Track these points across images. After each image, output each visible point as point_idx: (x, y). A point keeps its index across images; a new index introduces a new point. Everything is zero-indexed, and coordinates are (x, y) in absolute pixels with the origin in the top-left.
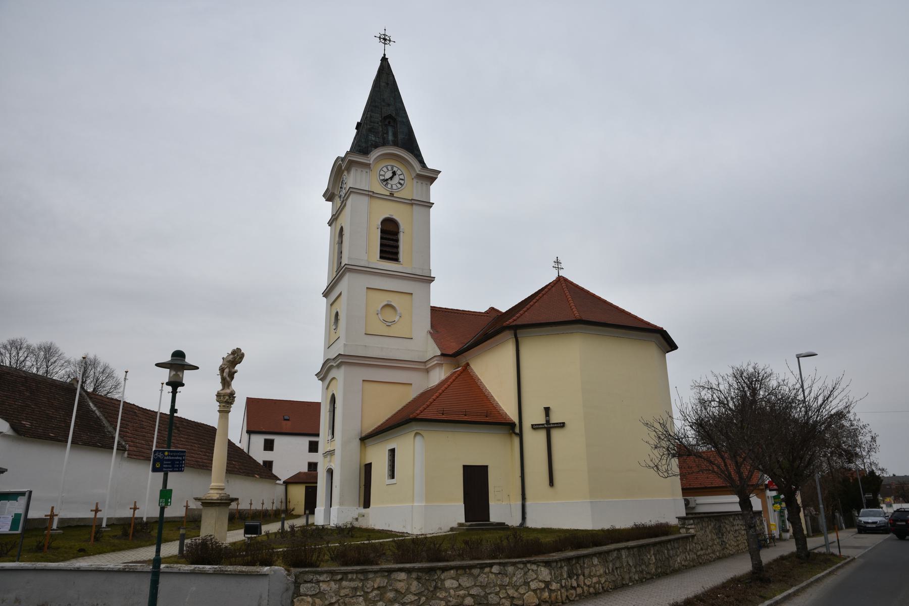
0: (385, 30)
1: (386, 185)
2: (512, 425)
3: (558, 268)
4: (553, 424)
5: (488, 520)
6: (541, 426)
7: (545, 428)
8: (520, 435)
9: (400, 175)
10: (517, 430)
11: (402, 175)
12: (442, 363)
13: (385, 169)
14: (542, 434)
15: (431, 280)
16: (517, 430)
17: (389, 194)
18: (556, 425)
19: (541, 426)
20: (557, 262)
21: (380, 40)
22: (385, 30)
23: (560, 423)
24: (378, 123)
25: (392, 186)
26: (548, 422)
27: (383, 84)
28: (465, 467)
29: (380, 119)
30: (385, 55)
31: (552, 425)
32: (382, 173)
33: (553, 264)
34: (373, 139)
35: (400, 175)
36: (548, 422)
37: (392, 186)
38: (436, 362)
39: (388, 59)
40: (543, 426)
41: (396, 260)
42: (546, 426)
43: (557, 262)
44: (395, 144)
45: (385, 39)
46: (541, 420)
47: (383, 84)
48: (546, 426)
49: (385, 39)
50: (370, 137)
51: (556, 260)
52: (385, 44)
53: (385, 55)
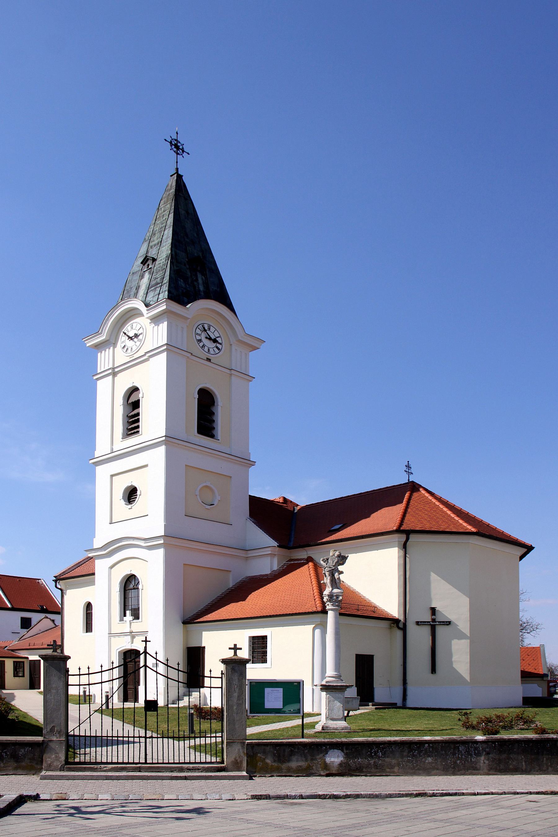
0: (177, 133)
3: (409, 472)
4: (439, 622)
6: (426, 623)
7: (430, 624)
8: (404, 629)
14: (426, 630)
15: (249, 463)
17: (206, 359)
18: (442, 623)
19: (426, 623)
20: (408, 466)
21: (171, 146)
22: (177, 133)
23: (447, 622)
24: (185, 265)
25: (209, 350)
26: (434, 620)
27: (183, 212)
29: (187, 260)
30: (177, 169)
31: (437, 623)
33: (405, 468)
34: (183, 285)
36: (434, 620)
37: (209, 350)
39: (183, 176)
40: (429, 623)
41: (212, 436)
42: (432, 623)
43: (408, 466)
44: (207, 296)
47: (183, 212)
50: (180, 282)
51: (407, 464)
52: (178, 154)
53: (177, 169)
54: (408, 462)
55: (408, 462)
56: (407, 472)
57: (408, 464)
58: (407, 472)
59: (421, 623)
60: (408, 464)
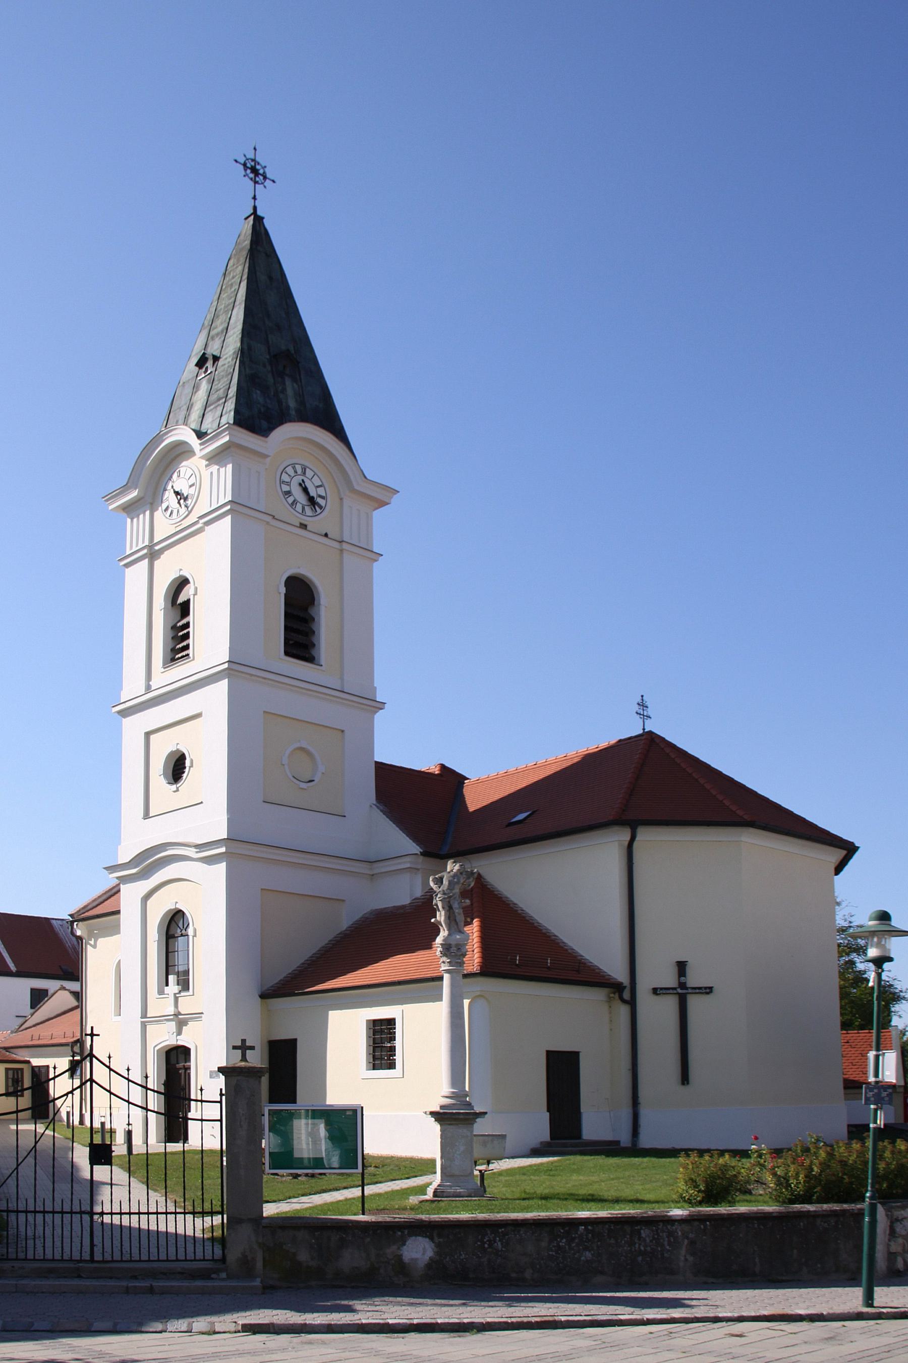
0: (255, 149)
1: (293, 504)
2: (616, 988)
3: (643, 715)
5: (579, 1136)
8: (632, 1003)
9: (318, 487)
10: (627, 995)
11: (322, 489)
12: (419, 867)
13: (290, 470)
14: (670, 1004)
16: (627, 995)
17: (298, 525)
18: (697, 991)
20: (642, 705)
21: (245, 170)
22: (255, 149)
23: (706, 988)
24: (264, 366)
27: (263, 278)
29: (268, 357)
30: (255, 208)
31: (690, 991)
32: (285, 478)
33: (636, 708)
34: (261, 400)
35: (318, 487)
36: (682, 985)
38: (408, 865)
40: (675, 992)
42: (679, 991)
43: (642, 705)
44: (303, 418)
45: (255, 171)
46: (669, 979)
47: (263, 278)
48: (679, 991)
49: (255, 171)
51: (639, 700)
52: (256, 182)
53: (255, 208)
54: (642, 696)
55: (642, 696)
56: (640, 714)
57: (642, 700)
58: (640, 714)
59: (661, 992)
60: (642, 700)
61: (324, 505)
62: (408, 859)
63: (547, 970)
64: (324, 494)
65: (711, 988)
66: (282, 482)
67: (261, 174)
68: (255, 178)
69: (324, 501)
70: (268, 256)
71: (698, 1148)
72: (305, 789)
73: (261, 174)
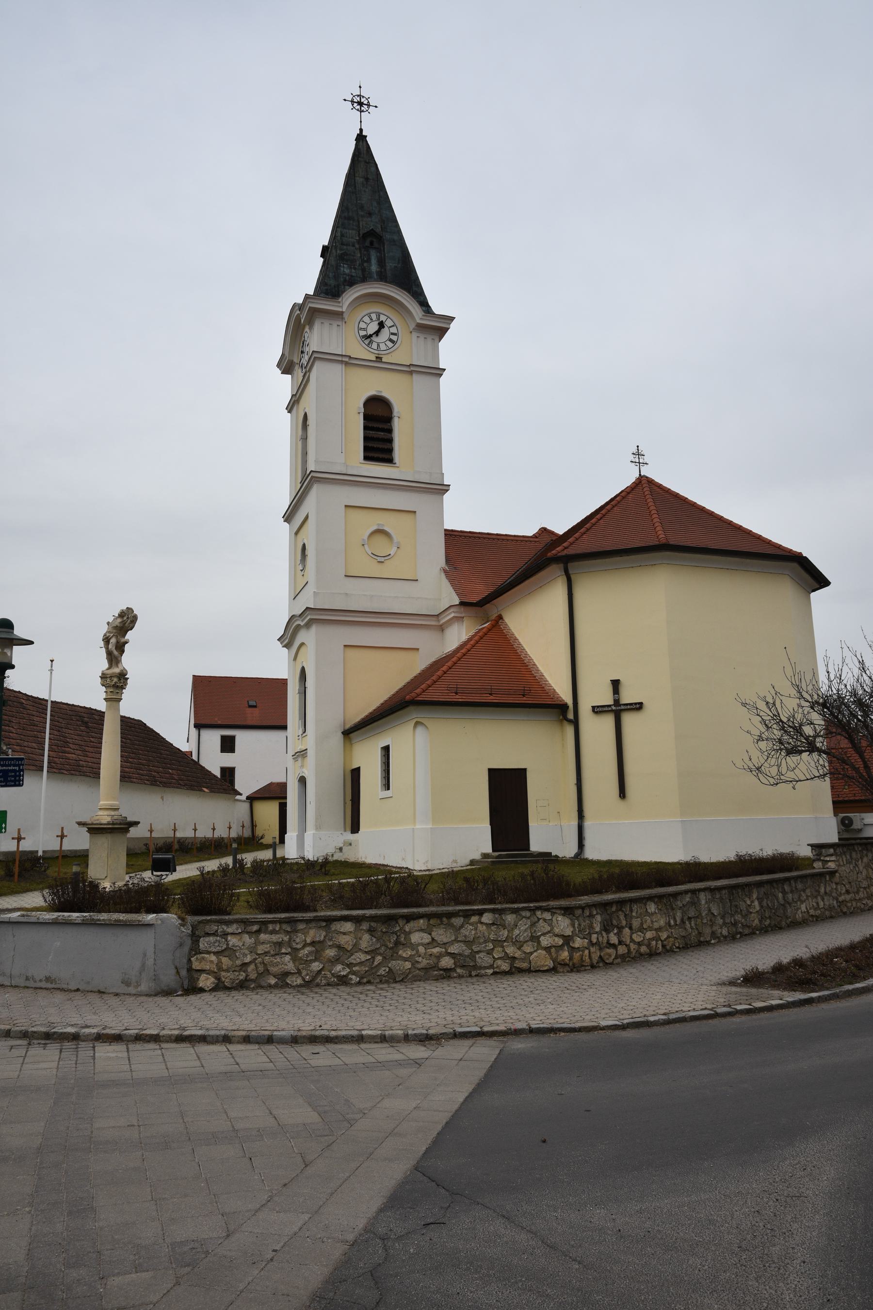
0: (360, 87)
1: (369, 344)
2: (562, 708)
3: (639, 463)
4: (625, 705)
5: (528, 849)
6: (606, 709)
7: (612, 711)
8: (576, 723)
9: (390, 327)
10: (571, 716)
11: (394, 328)
12: (463, 615)
13: (367, 319)
14: (609, 721)
15: (442, 489)
16: (571, 716)
17: (375, 359)
18: (629, 707)
19: (606, 709)
20: (638, 454)
22: (360, 87)
23: (636, 704)
24: (353, 246)
25: (378, 345)
26: (617, 702)
27: (359, 180)
28: (491, 771)
29: (357, 238)
30: (361, 130)
31: (623, 707)
32: (362, 325)
33: (632, 458)
34: (347, 271)
35: (390, 327)
36: (617, 702)
37: (378, 345)
38: (453, 615)
39: (366, 136)
40: (610, 709)
41: (390, 460)
42: (614, 708)
43: (638, 454)
44: (382, 277)
45: (360, 104)
46: (607, 699)
47: (359, 180)
48: (614, 708)
49: (360, 104)
50: (342, 269)
51: (635, 451)
52: (361, 111)
53: (361, 130)
54: (638, 447)
55: (638, 447)
56: (635, 462)
57: (638, 450)
58: (635, 462)
59: (598, 710)
60: (638, 450)
61: (396, 340)
62: (452, 610)
63: (522, 696)
64: (395, 331)
65: (641, 704)
66: (360, 329)
67: (356, 102)
68: (361, 109)
69: (396, 337)
70: (367, 163)
71: (265, 994)
72: (383, 562)
73: (356, 102)
